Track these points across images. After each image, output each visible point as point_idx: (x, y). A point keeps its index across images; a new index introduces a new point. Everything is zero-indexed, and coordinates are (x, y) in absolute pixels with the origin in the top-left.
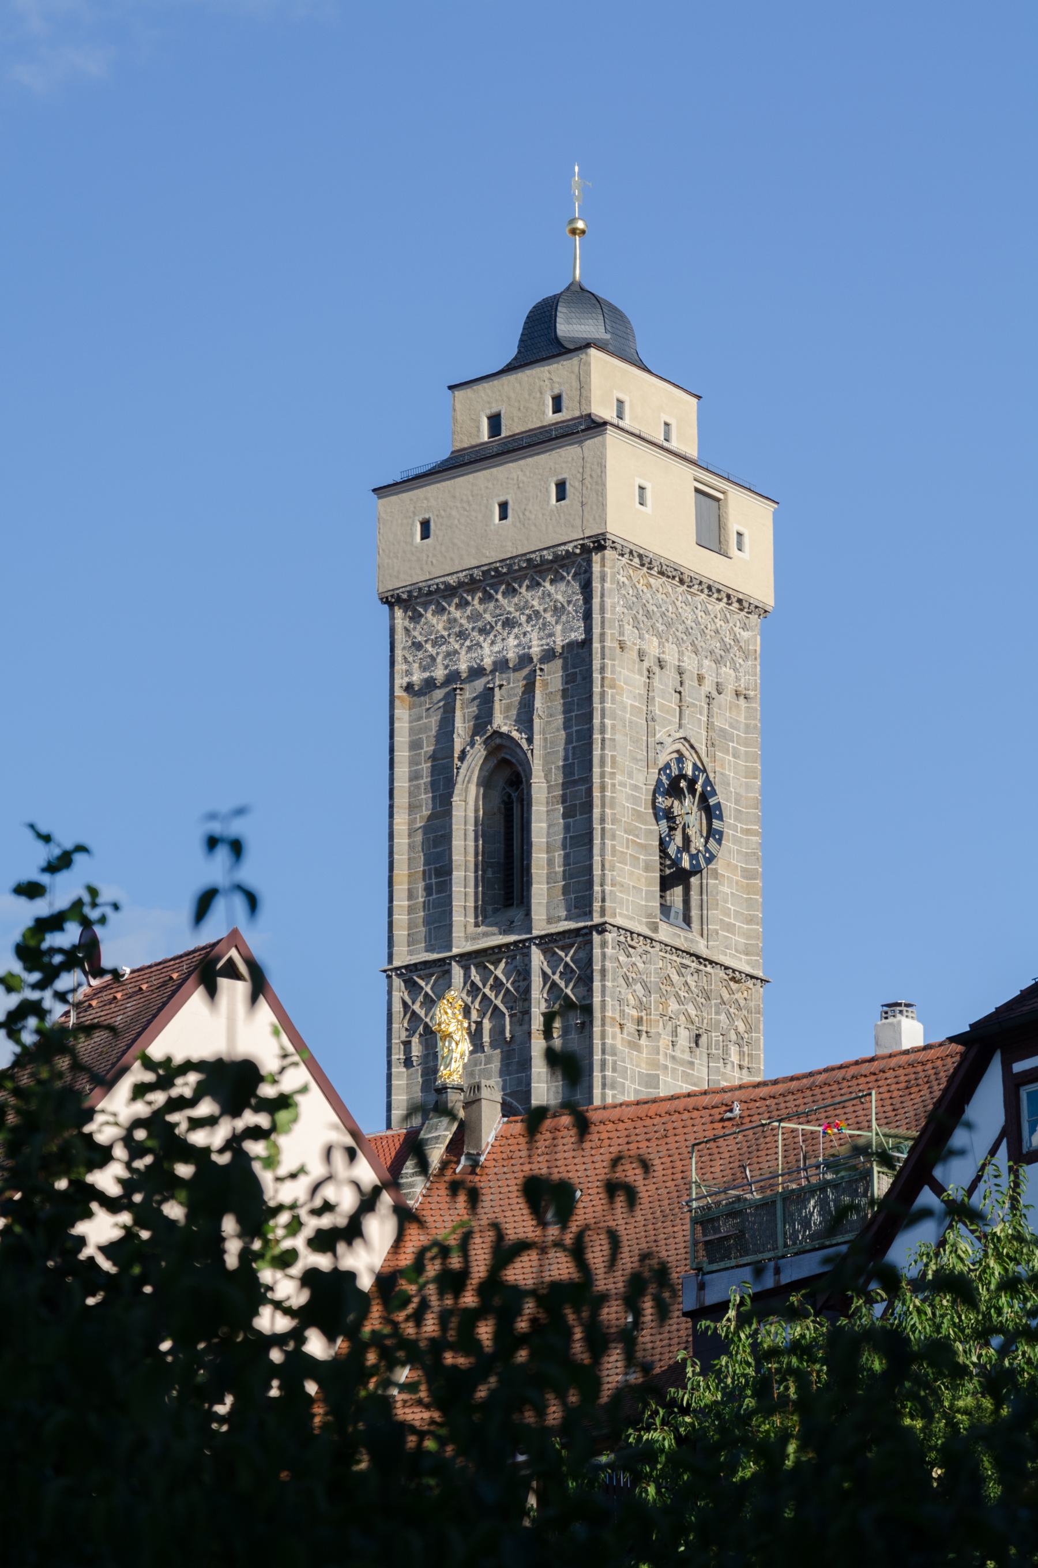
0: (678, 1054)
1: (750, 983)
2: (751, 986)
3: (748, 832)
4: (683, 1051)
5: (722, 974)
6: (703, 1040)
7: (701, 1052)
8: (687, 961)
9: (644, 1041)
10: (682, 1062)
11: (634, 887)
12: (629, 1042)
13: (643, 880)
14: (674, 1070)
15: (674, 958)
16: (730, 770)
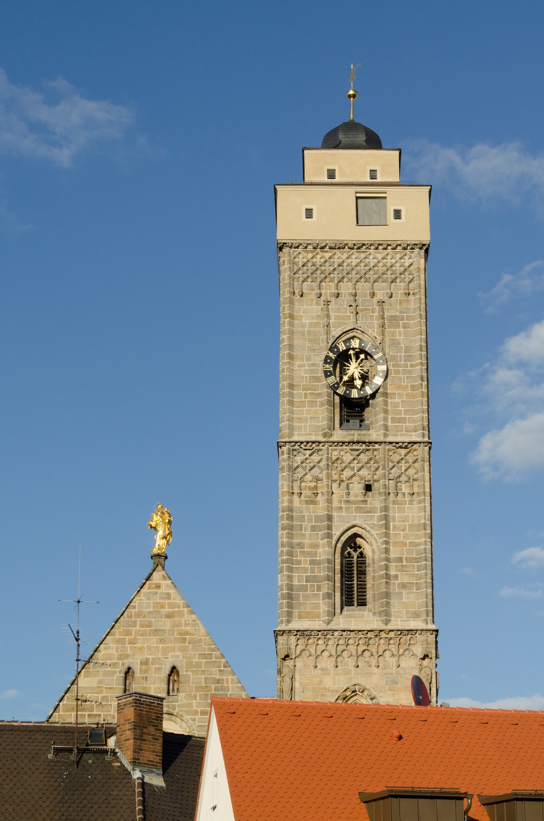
0: (351, 498)
1: (416, 446)
2: (417, 448)
3: (416, 365)
4: (357, 496)
5: (390, 447)
6: (375, 486)
7: (373, 494)
8: (355, 447)
9: (319, 498)
10: (355, 503)
11: (311, 418)
12: (307, 502)
13: (320, 412)
14: (347, 508)
15: (344, 447)
16: (400, 336)
